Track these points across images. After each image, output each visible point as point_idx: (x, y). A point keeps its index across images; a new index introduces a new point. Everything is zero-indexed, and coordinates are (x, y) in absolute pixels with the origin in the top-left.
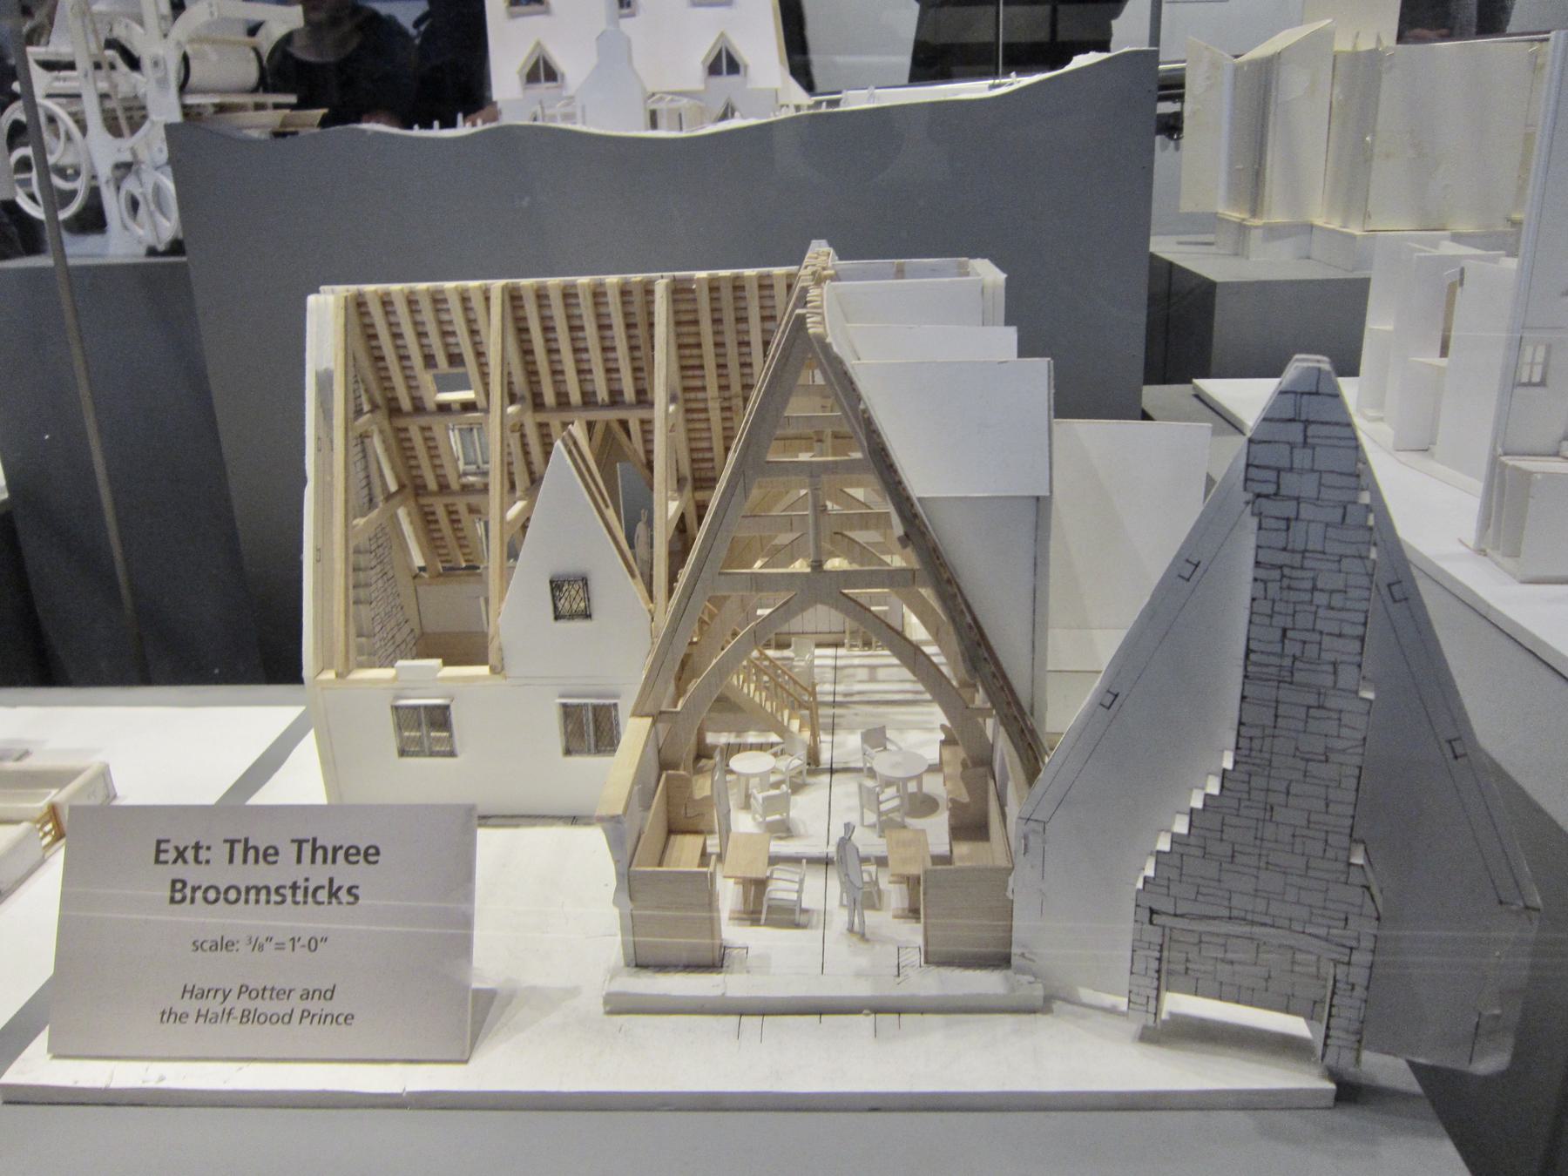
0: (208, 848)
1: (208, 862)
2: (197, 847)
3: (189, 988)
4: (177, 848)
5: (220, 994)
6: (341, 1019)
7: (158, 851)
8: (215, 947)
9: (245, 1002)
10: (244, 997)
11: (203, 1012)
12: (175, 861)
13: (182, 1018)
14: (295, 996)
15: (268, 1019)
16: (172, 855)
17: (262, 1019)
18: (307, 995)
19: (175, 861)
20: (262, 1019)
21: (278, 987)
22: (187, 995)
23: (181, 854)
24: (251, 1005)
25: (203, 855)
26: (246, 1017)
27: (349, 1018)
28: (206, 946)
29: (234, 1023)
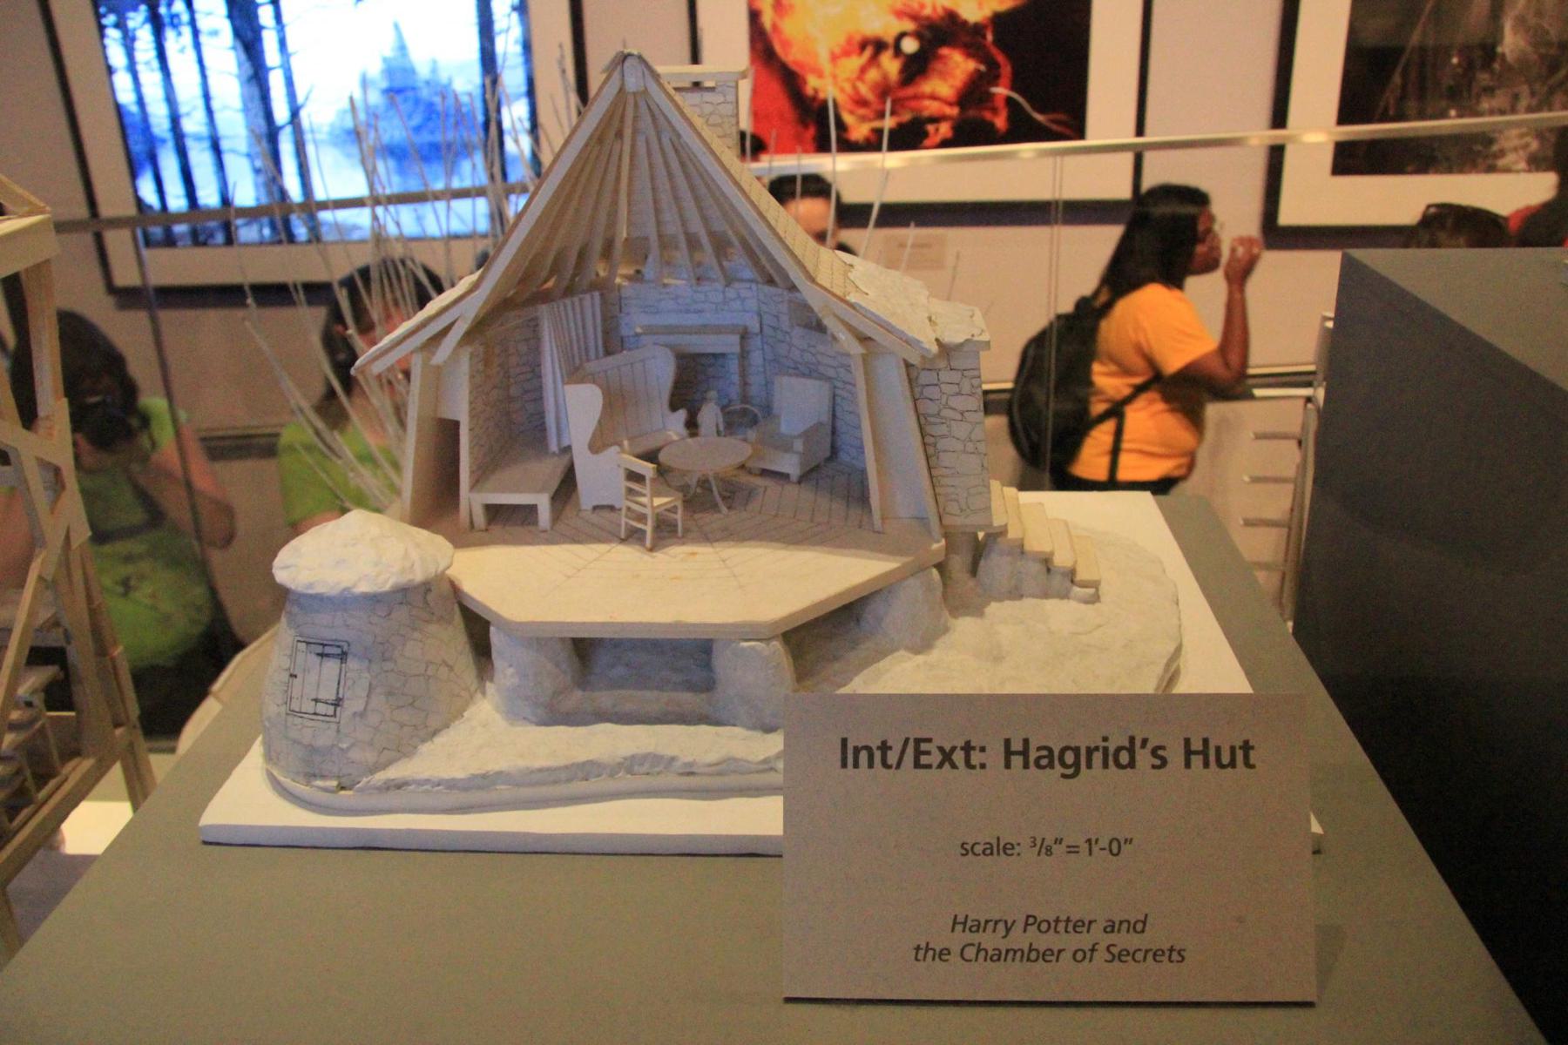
1: (983, 766)
2: (968, 748)
3: (961, 919)
4: (941, 749)
5: (1001, 926)
12: (940, 766)
16: (936, 758)
18: (1111, 928)
19: (940, 766)
21: (1074, 918)
22: (959, 928)
23: (947, 757)
25: (976, 758)
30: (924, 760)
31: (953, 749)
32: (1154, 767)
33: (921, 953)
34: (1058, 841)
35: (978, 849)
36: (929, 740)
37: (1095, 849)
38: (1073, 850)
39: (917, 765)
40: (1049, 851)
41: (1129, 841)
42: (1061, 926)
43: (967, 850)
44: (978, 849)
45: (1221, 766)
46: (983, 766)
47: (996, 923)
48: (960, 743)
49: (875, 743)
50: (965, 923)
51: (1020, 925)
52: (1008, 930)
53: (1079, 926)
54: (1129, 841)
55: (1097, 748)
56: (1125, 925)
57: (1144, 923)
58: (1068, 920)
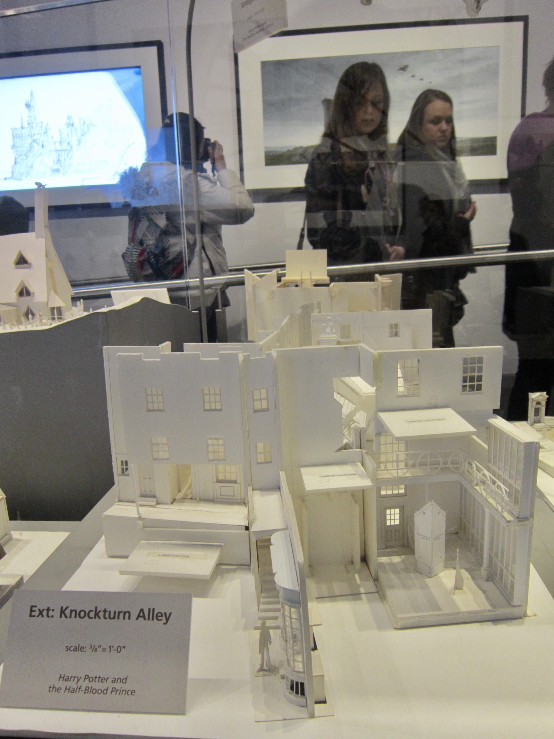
0: (53, 610)
2: (48, 610)
4: (39, 610)
5: (76, 679)
6: (130, 693)
7: (32, 611)
9: (87, 683)
10: (87, 680)
11: (68, 688)
12: (38, 616)
13: (58, 690)
14: (109, 681)
15: (97, 691)
16: (37, 613)
17: (94, 691)
18: (114, 681)
19: (38, 616)
20: (94, 691)
21: (102, 677)
22: (61, 679)
23: (41, 613)
24: (90, 685)
25: (51, 613)
26: (87, 690)
27: (133, 692)
29: (82, 693)
30: (33, 614)
31: (43, 610)
33: (51, 689)
34: (100, 646)
35: (72, 649)
36: (36, 606)
37: (112, 649)
38: (104, 650)
39: (31, 616)
40: (96, 650)
41: (124, 647)
42: (97, 679)
43: (68, 649)
44: (72, 649)
45: (110, 618)
47: (75, 677)
48: (46, 608)
51: (83, 679)
52: (78, 681)
53: (103, 680)
54: (124, 647)
55: (122, 612)
56: (119, 680)
57: (126, 679)
58: (99, 678)
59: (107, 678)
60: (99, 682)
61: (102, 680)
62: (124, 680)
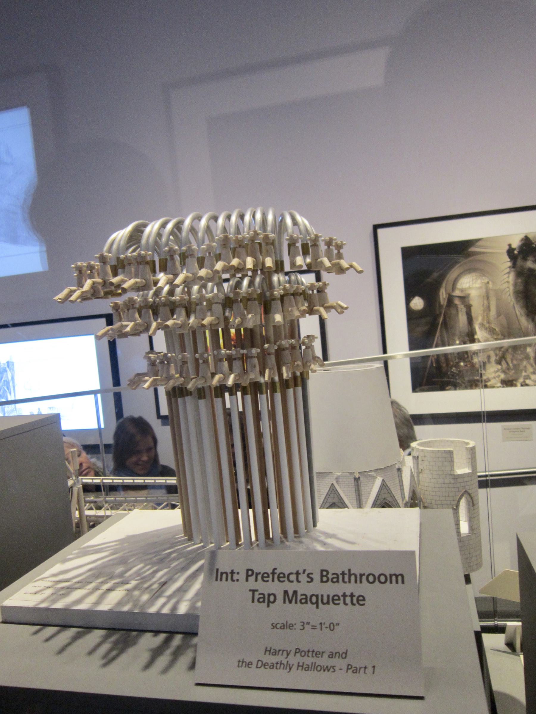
3: (269, 649)
5: (285, 653)
8: (283, 627)
10: (298, 655)
14: (326, 655)
18: (332, 655)
21: (316, 651)
22: (268, 653)
28: (278, 626)
32: (308, 582)
42: (310, 654)
46: (238, 580)
47: (283, 651)
49: (229, 571)
50: (270, 651)
52: (288, 655)
53: (318, 654)
56: (338, 655)
57: (346, 654)
58: (313, 651)
59: (323, 652)
60: (313, 657)
61: (316, 654)
62: (344, 655)
